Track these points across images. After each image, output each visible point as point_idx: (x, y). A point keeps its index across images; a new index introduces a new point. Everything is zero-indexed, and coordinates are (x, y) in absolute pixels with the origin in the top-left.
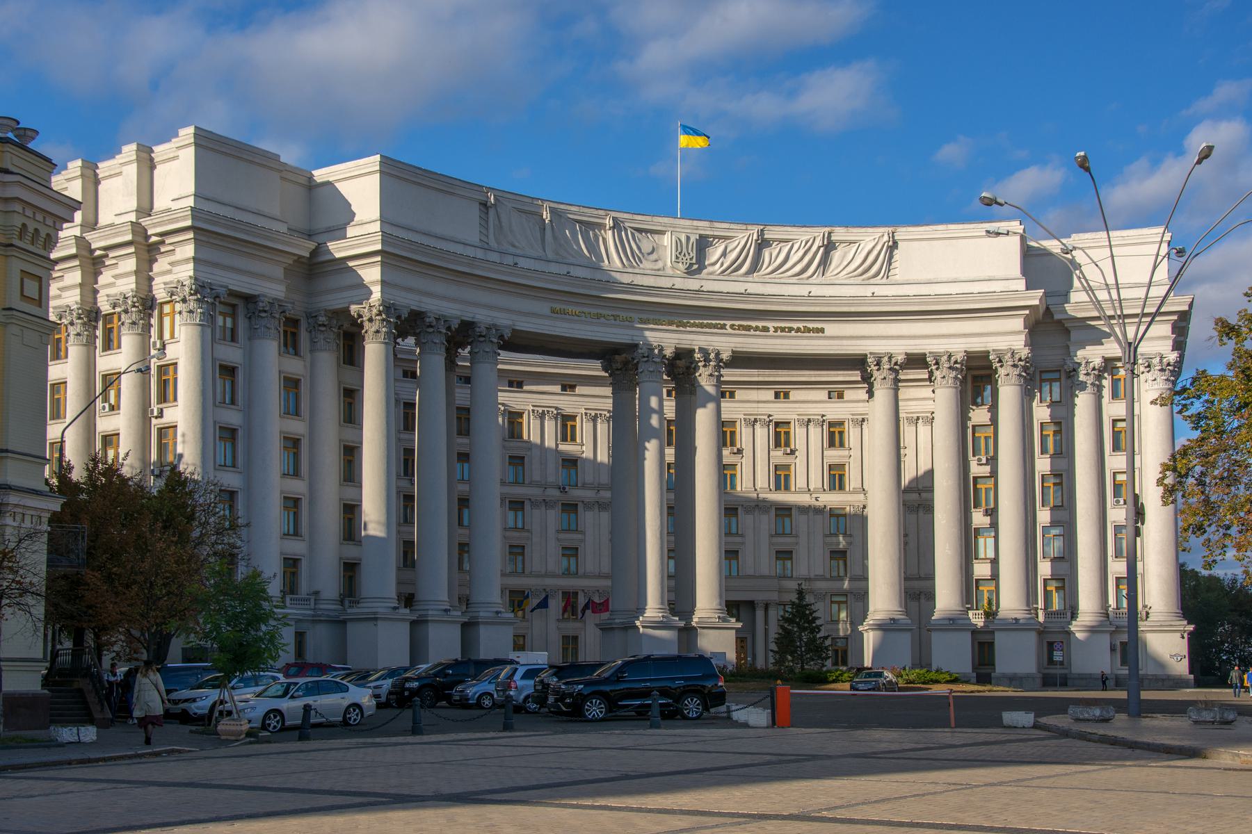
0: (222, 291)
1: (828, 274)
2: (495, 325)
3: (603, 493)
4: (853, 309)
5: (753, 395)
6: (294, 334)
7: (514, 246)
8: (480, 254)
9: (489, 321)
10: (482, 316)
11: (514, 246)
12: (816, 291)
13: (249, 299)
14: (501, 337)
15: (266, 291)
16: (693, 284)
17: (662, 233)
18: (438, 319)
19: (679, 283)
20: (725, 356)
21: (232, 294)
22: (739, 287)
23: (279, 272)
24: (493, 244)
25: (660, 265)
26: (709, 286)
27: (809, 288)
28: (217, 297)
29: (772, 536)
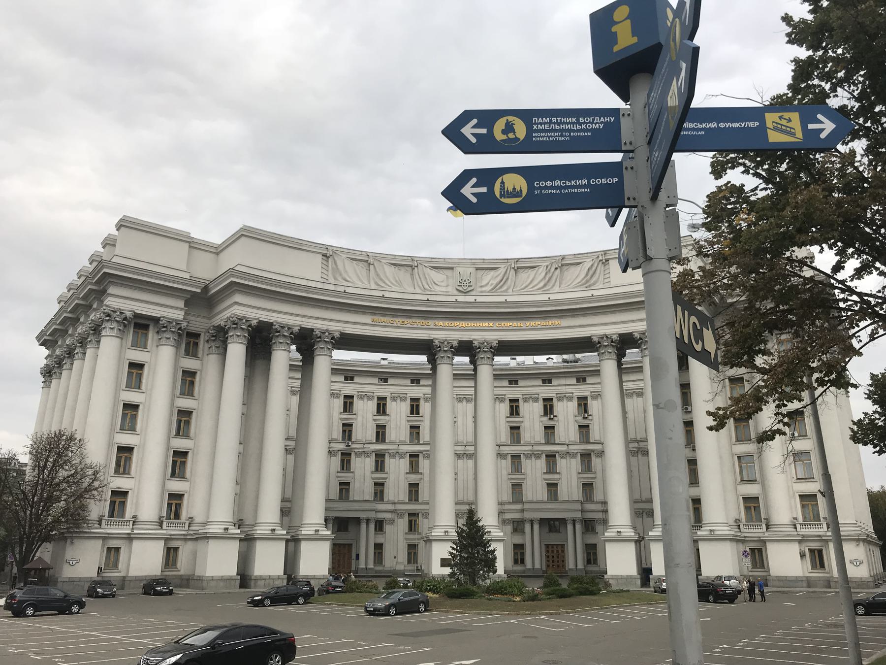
0: (129, 314)
1: (563, 286)
2: (327, 330)
3: (468, 448)
4: (578, 306)
5: (563, 381)
6: (196, 344)
7: (346, 281)
8: (319, 285)
9: (325, 328)
10: (317, 325)
11: (346, 281)
12: (553, 297)
13: (156, 320)
14: (333, 338)
15: (166, 314)
16: (470, 299)
17: (452, 268)
18: (283, 327)
19: (461, 298)
20: (494, 344)
21: (137, 316)
22: (502, 299)
23: (181, 304)
24: (331, 280)
25: (450, 289)
26: (479, 299)
27: (549, 296)
28: (125, 319)
29: (579, 473)
